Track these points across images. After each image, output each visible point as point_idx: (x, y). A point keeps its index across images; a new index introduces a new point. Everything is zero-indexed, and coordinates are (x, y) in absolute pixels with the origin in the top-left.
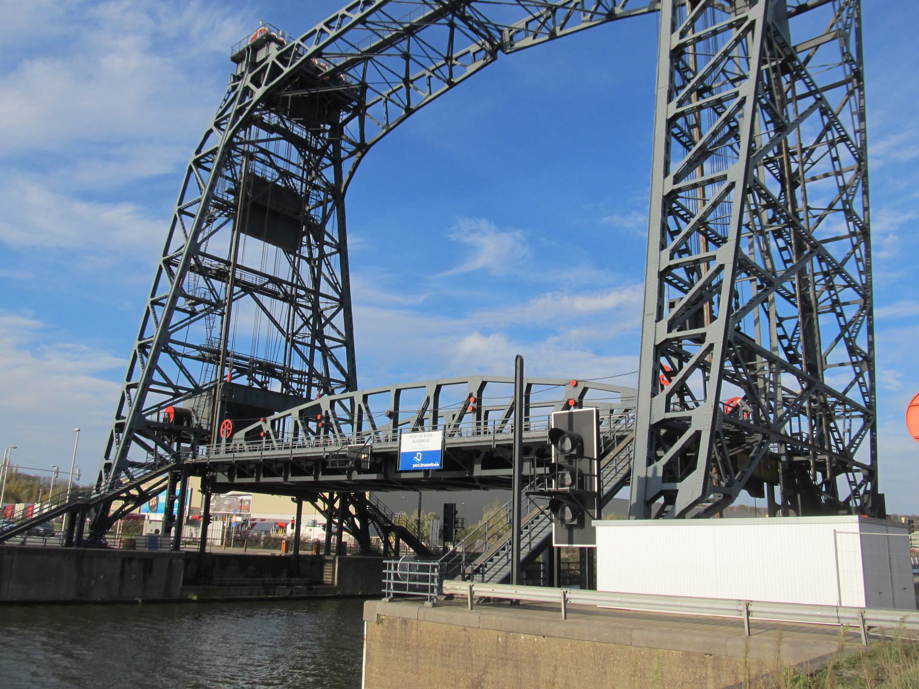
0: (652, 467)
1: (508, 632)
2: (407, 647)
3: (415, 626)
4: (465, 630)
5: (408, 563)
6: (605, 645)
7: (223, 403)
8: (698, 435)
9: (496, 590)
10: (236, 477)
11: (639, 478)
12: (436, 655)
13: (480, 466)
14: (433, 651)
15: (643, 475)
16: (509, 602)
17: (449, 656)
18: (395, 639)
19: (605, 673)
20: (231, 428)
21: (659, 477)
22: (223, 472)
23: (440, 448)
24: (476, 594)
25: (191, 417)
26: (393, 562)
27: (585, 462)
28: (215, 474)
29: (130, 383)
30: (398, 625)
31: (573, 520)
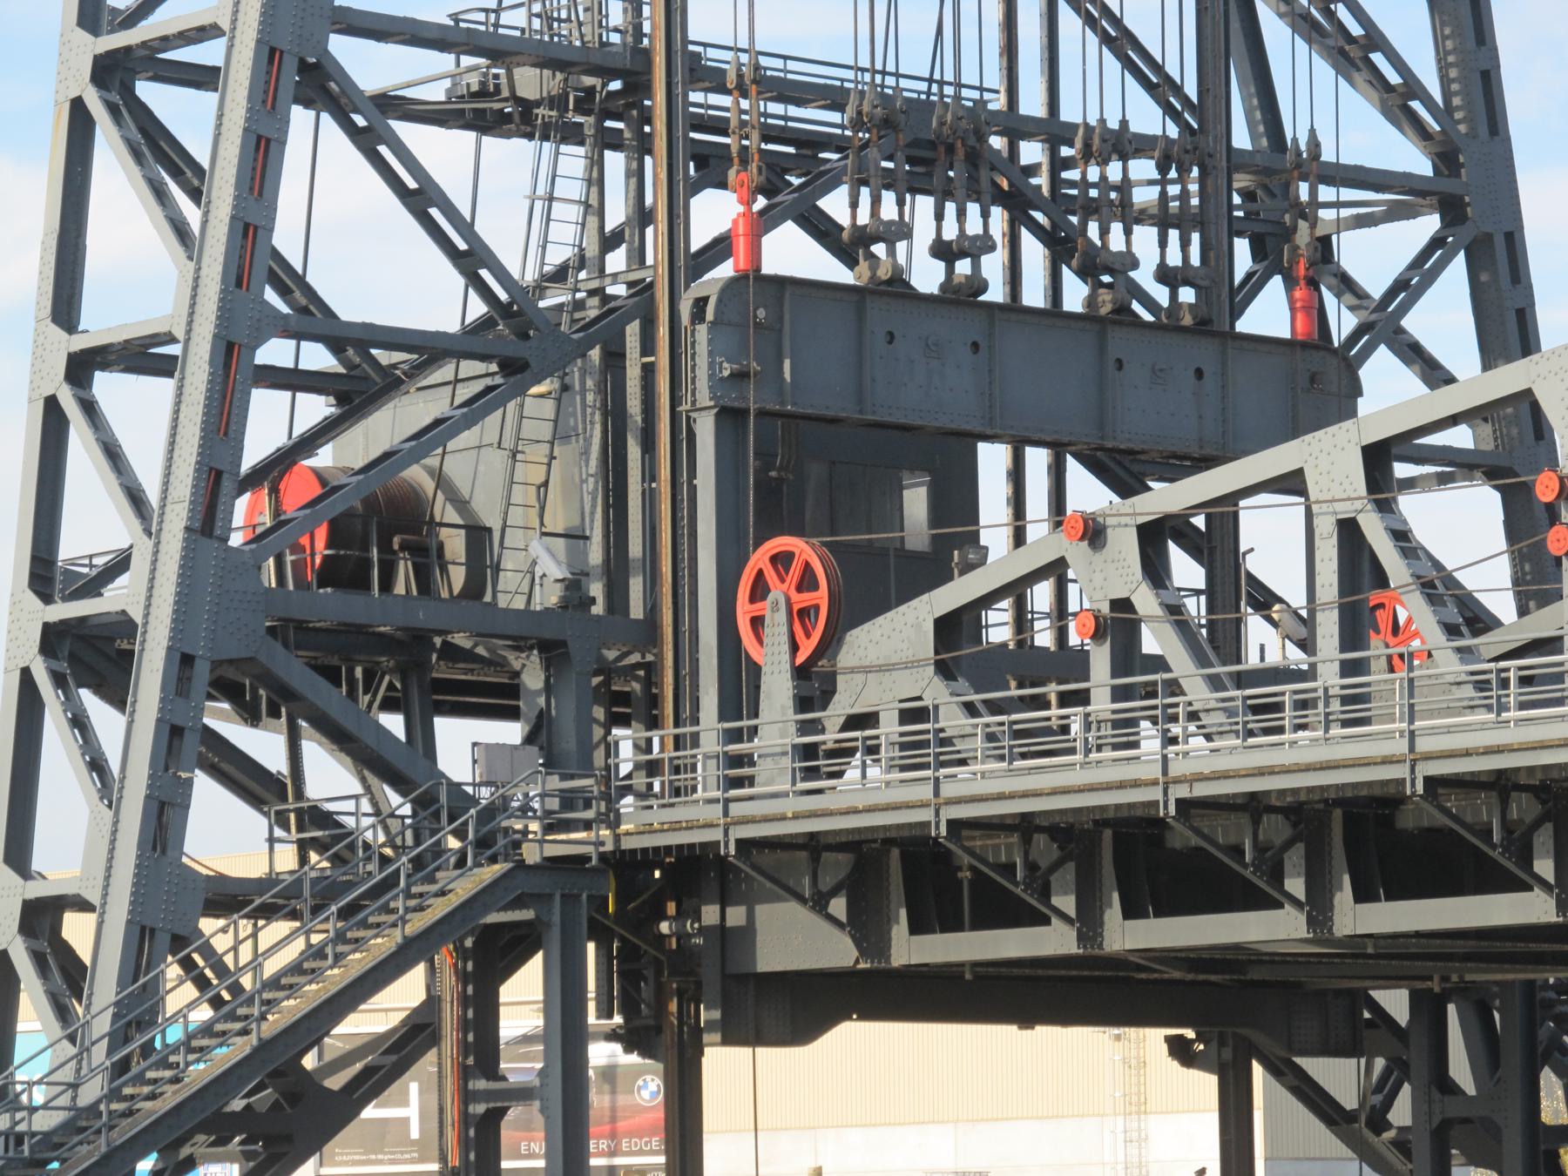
7: (730, 417)
10: (900, 930)
20: (821, 597)
22: (819, 904)
25: (434, 525)
28: (736, 916)
29: (79, 343)
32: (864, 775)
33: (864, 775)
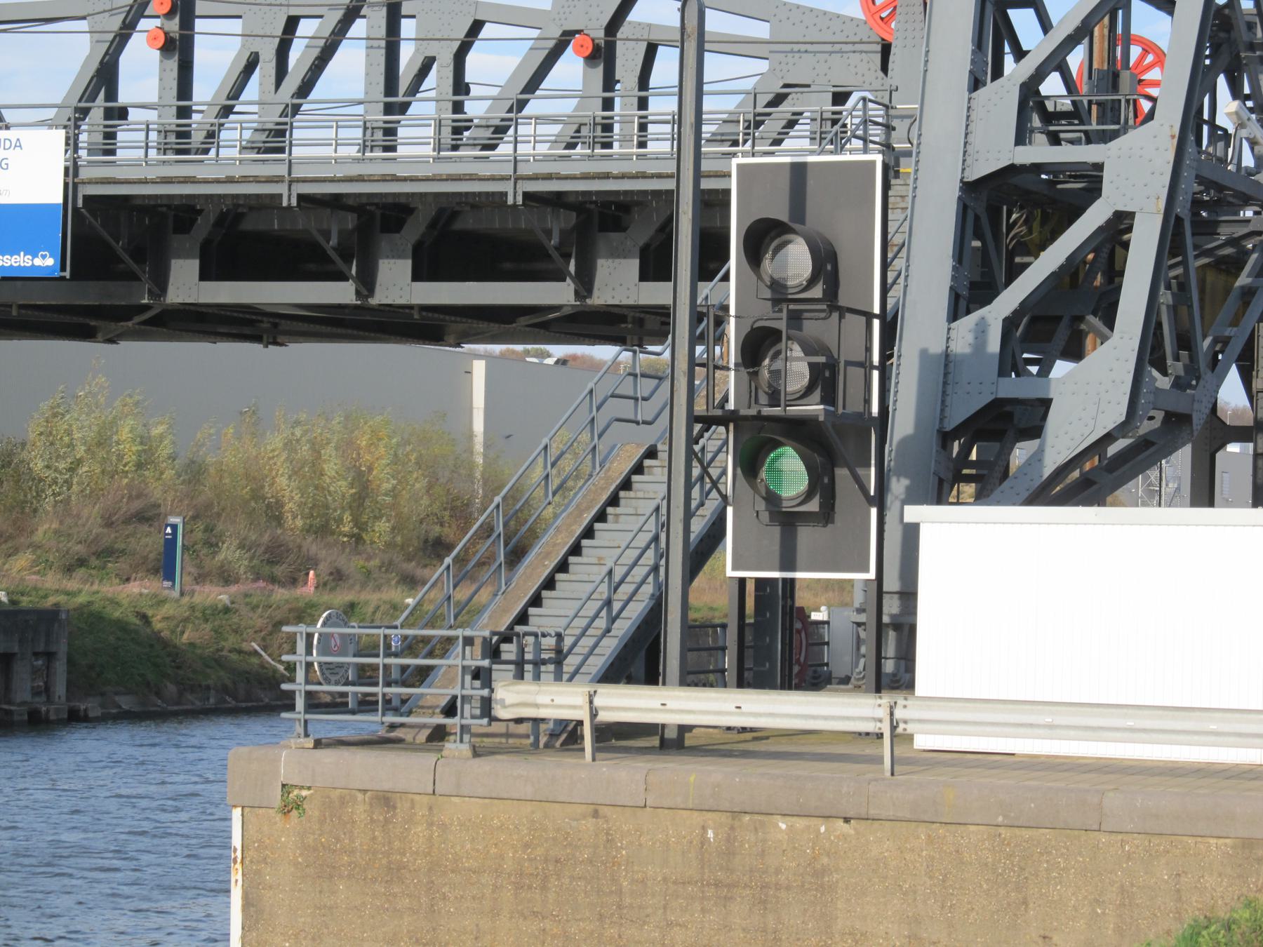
0: (968, 322)
1: (736, 814)
2: (395, 872)
3: (421, 812)
4: (596, 814)
5: (381, 631)
6: (1026, 833)
8: (1120, 224)
9: (671, 705)
11: (924, 354)
12: (496, 888)
13: (194, 265)
14: (485, 879)
15: (937, 348)
16: (655, 741)
17: (544, 888)
18: (352, 852)
19: (1025, 902)
21: (992, 355)
23: (59, 199)
24: (604, 717)
26: (302, 628)
27: (854, 323)
30: (360, 811)
31: (808, 496)
32: (146, 155)
33: (146, 155)
